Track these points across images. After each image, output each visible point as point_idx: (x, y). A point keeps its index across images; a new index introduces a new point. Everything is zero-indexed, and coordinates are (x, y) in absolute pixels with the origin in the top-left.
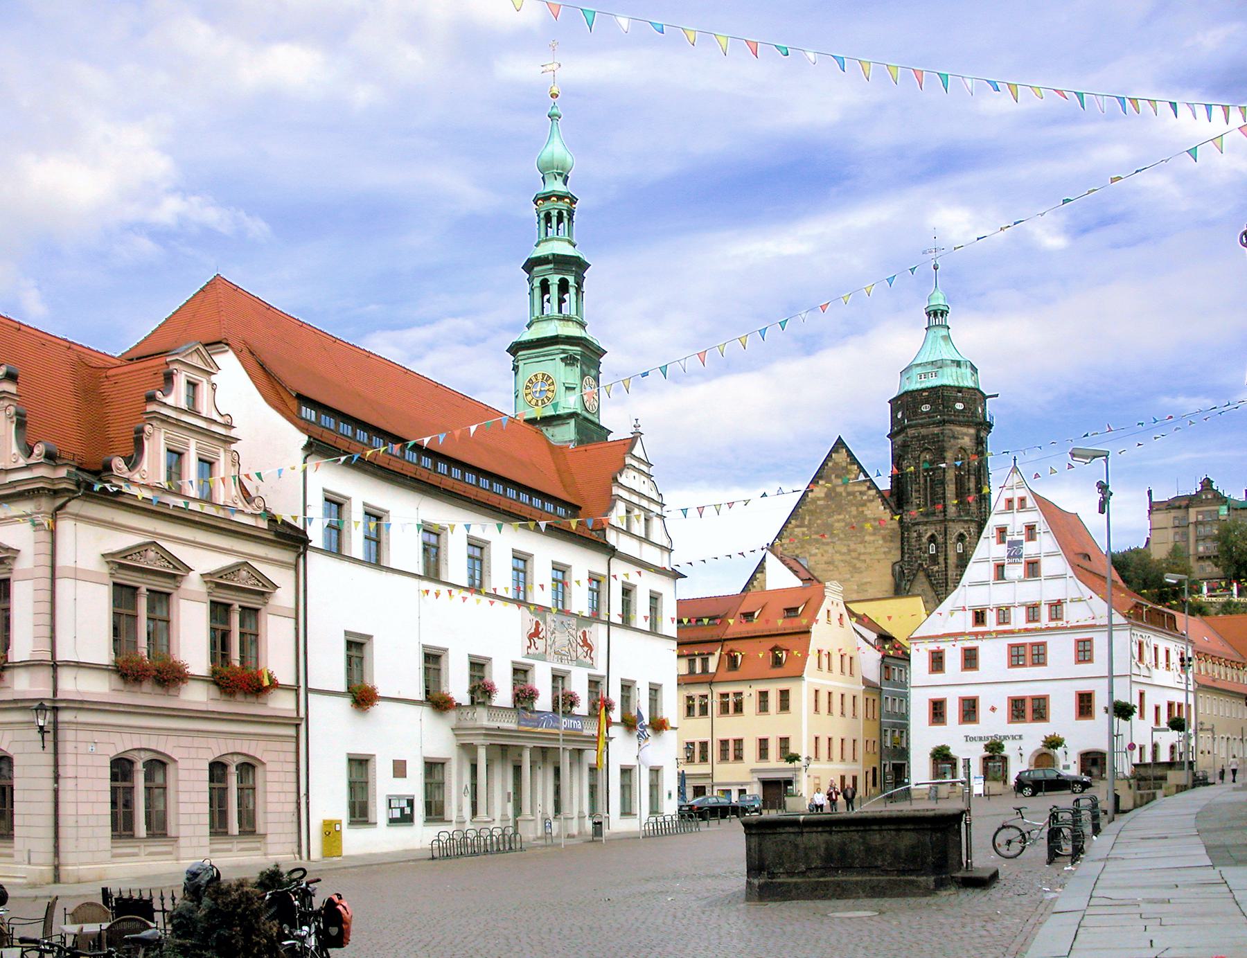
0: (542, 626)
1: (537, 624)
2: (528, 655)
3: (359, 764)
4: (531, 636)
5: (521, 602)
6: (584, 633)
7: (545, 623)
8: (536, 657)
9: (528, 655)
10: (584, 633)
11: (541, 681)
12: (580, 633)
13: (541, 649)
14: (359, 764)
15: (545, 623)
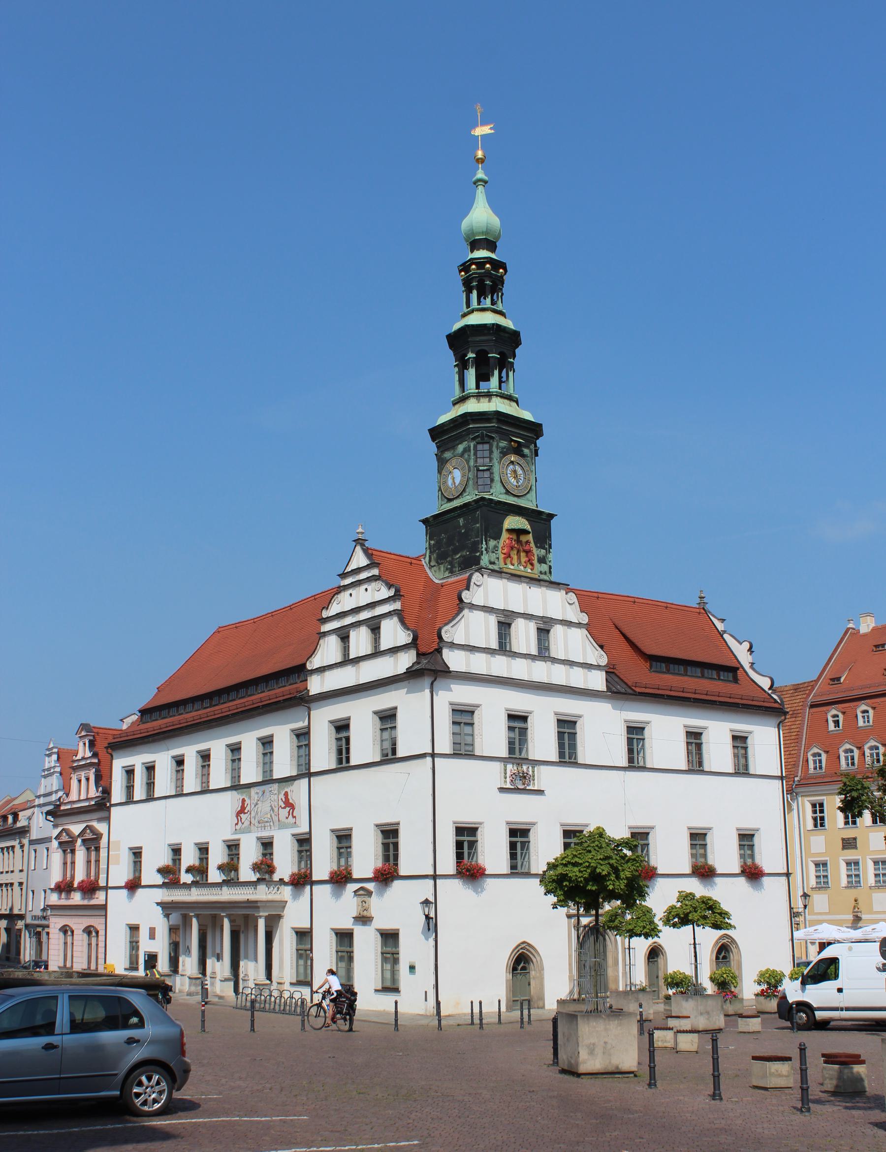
0: (247, 801)
1: (244, 801)
2: (236, 831)
3: (134, 929)
4: (238, 814)
5: (236, 787)
6: (286, 794)
7: (250, 797)
8: (243, 832)
9: (236, 831)
10: (286, 794)
11: (249, 854)
12: (282, 796)
13: (247, 823)
14: (134, 929)
15: (250, 797)
